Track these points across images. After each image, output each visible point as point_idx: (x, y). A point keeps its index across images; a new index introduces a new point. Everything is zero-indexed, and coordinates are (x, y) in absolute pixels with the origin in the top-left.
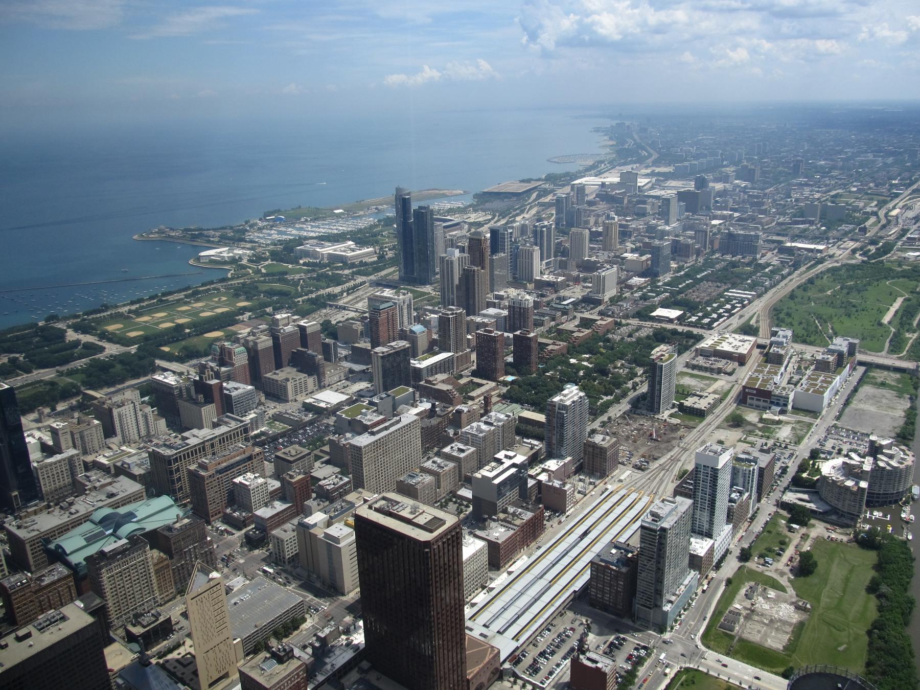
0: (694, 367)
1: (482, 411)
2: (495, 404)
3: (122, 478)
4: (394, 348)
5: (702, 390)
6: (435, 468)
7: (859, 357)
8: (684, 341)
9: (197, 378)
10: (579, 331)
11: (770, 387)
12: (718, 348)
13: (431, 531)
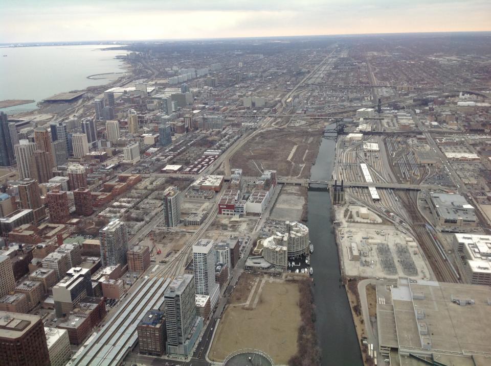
1: (57, 245)
2: (66, 238)
5: (196, 210)
6: (26, 288)
8: (182, 183)
13: (21, 330)
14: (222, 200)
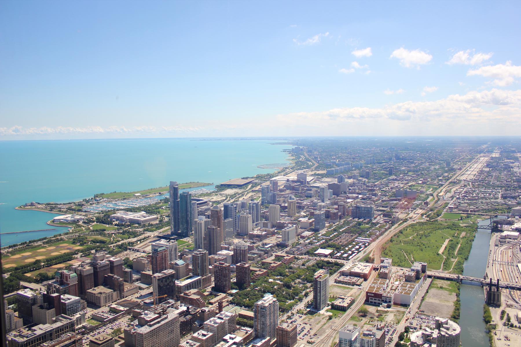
0: (340, 282)
1: (218, 311)
2: (225, 307)
4: (166, 274)
7: (428, 273)
8: (333, 267)
9: (46, 293)
10: (274, 263)
11: (381, 292)
12: (352, 270)
14: (370, 287)
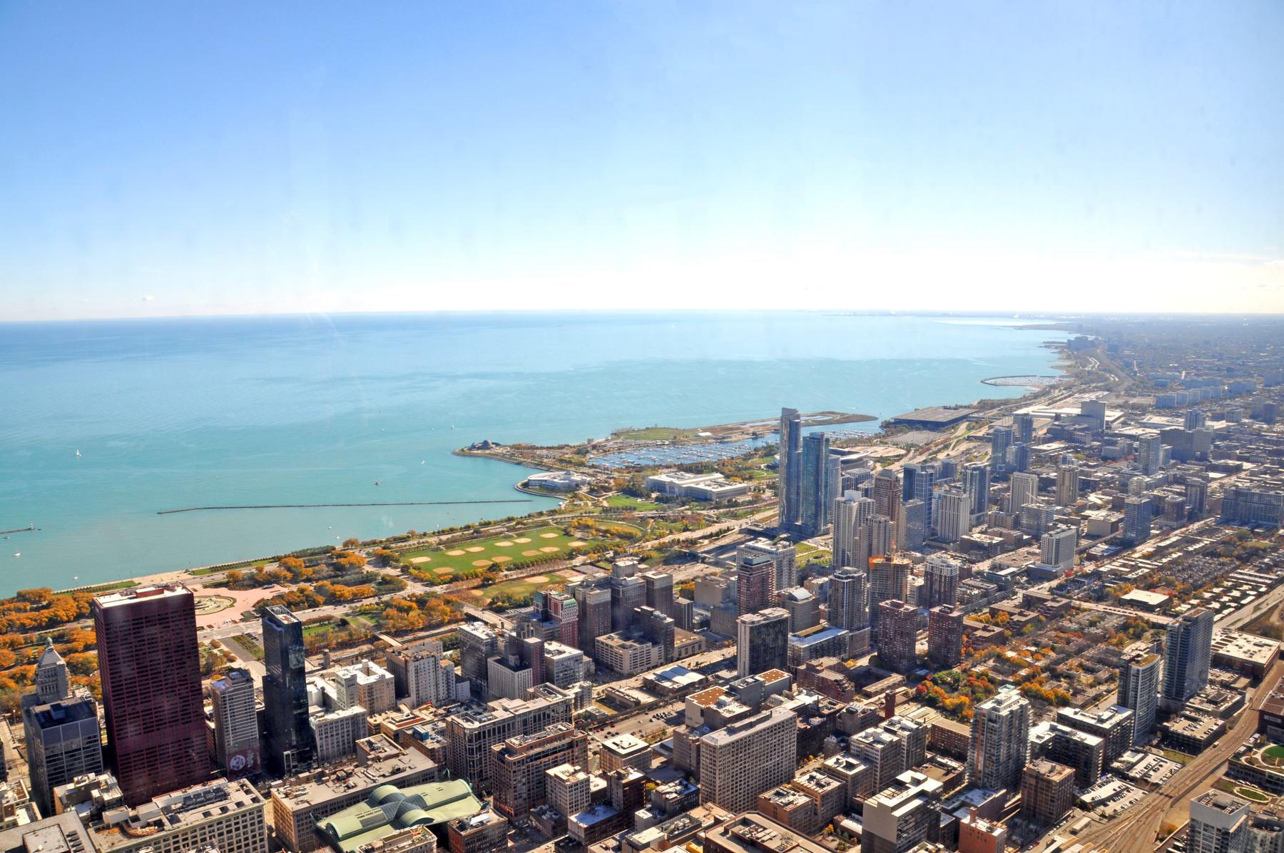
1: (883, 714)
3: (412, 751)
9: (514, 634)
10: (1021, 614)
12: (1221, 651)
